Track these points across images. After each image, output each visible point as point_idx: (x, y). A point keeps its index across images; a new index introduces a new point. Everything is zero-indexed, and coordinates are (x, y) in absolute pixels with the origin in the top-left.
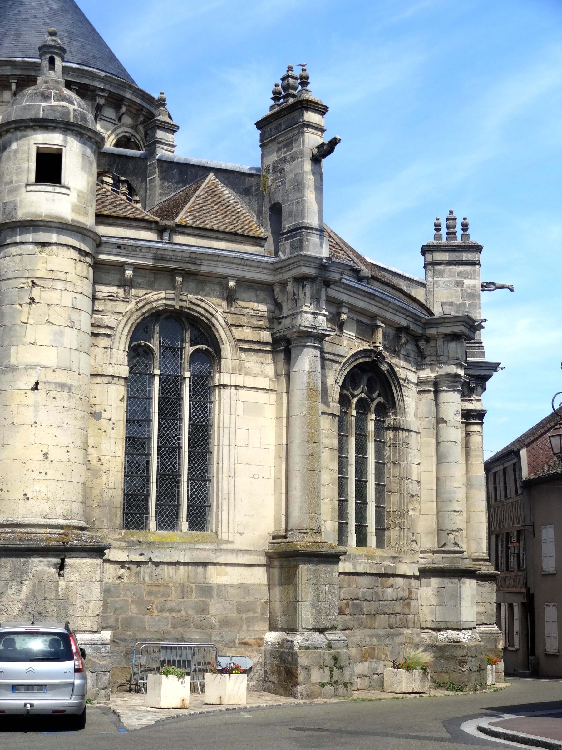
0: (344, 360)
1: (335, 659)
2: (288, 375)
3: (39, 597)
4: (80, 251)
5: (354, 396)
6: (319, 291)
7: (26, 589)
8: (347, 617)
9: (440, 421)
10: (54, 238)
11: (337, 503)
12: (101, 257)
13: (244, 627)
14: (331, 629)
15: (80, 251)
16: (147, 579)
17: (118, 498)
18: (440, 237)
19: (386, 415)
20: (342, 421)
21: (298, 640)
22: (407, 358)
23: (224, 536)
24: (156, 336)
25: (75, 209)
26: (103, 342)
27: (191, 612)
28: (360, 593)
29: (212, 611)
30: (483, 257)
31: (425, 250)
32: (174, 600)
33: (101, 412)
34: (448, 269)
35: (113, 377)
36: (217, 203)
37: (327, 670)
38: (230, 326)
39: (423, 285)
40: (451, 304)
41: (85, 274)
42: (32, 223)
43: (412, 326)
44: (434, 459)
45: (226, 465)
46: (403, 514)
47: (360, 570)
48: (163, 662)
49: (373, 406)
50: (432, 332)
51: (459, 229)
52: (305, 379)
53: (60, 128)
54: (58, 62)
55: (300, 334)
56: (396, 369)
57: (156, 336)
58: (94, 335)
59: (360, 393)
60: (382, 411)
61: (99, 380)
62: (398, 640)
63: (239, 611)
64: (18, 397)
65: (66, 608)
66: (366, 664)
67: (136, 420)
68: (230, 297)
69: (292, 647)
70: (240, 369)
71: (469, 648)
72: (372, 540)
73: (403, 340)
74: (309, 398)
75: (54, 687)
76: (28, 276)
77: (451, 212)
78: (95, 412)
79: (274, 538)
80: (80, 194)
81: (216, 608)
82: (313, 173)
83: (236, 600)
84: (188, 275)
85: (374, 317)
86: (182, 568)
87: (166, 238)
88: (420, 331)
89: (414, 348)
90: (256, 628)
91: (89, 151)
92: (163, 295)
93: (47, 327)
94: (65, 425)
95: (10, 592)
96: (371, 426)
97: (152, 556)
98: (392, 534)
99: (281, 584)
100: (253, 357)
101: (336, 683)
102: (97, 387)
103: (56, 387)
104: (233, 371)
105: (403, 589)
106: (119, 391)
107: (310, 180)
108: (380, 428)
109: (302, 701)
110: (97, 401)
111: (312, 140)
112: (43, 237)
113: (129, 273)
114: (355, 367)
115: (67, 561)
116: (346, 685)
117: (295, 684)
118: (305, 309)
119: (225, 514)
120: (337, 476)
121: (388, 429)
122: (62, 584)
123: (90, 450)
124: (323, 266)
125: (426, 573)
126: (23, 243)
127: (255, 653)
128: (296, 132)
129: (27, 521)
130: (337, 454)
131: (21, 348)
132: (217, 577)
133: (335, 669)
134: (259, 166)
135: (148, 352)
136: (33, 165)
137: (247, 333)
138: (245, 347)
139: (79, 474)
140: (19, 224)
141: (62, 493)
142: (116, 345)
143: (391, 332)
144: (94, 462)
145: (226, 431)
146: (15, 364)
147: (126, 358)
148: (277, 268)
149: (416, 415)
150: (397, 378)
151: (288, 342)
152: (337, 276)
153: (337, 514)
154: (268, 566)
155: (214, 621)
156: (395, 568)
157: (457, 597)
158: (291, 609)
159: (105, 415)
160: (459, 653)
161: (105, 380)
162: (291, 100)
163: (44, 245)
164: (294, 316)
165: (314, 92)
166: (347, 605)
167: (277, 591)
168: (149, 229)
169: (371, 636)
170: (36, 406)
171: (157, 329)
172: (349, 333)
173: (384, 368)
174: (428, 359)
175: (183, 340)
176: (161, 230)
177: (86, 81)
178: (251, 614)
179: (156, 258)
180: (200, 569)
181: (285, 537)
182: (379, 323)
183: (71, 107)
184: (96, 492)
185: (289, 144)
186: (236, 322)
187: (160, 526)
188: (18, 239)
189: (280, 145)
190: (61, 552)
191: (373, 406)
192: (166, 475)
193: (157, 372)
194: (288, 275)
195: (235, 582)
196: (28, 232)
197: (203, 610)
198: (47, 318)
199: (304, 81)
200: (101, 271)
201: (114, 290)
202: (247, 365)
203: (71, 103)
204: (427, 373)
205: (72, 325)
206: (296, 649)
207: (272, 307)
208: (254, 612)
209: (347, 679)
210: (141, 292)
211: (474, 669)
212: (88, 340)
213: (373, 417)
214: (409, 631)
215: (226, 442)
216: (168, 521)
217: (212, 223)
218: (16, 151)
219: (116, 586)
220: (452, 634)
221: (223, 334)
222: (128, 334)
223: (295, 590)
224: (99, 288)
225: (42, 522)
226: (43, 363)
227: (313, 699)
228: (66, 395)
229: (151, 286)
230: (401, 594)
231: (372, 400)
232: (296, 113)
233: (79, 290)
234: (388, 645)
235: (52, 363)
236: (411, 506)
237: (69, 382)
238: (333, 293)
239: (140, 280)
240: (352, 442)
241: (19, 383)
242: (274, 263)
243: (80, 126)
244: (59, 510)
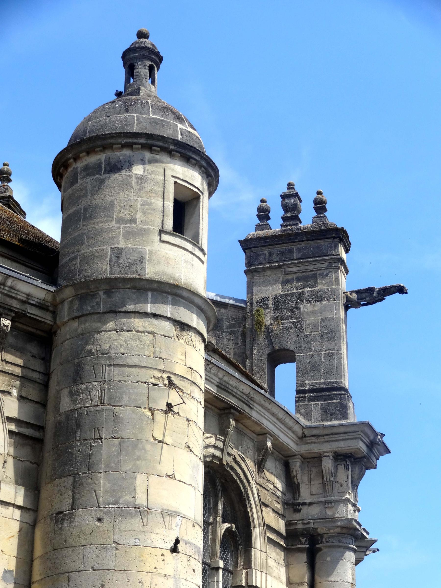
42: (175, 291)
55: (344, 531)
76: (162, 368)
126: (155, 316)
128: (323, 266)
131: (153, 479)
140: (155, 286)
146: (145, 503)
185: (309, 279)
188: (150, 308)
189: (290, 277)
194: (328, 448)
196: (164, 302)
198: (186, 440)
218: (141, 179)
241: (153, 536)
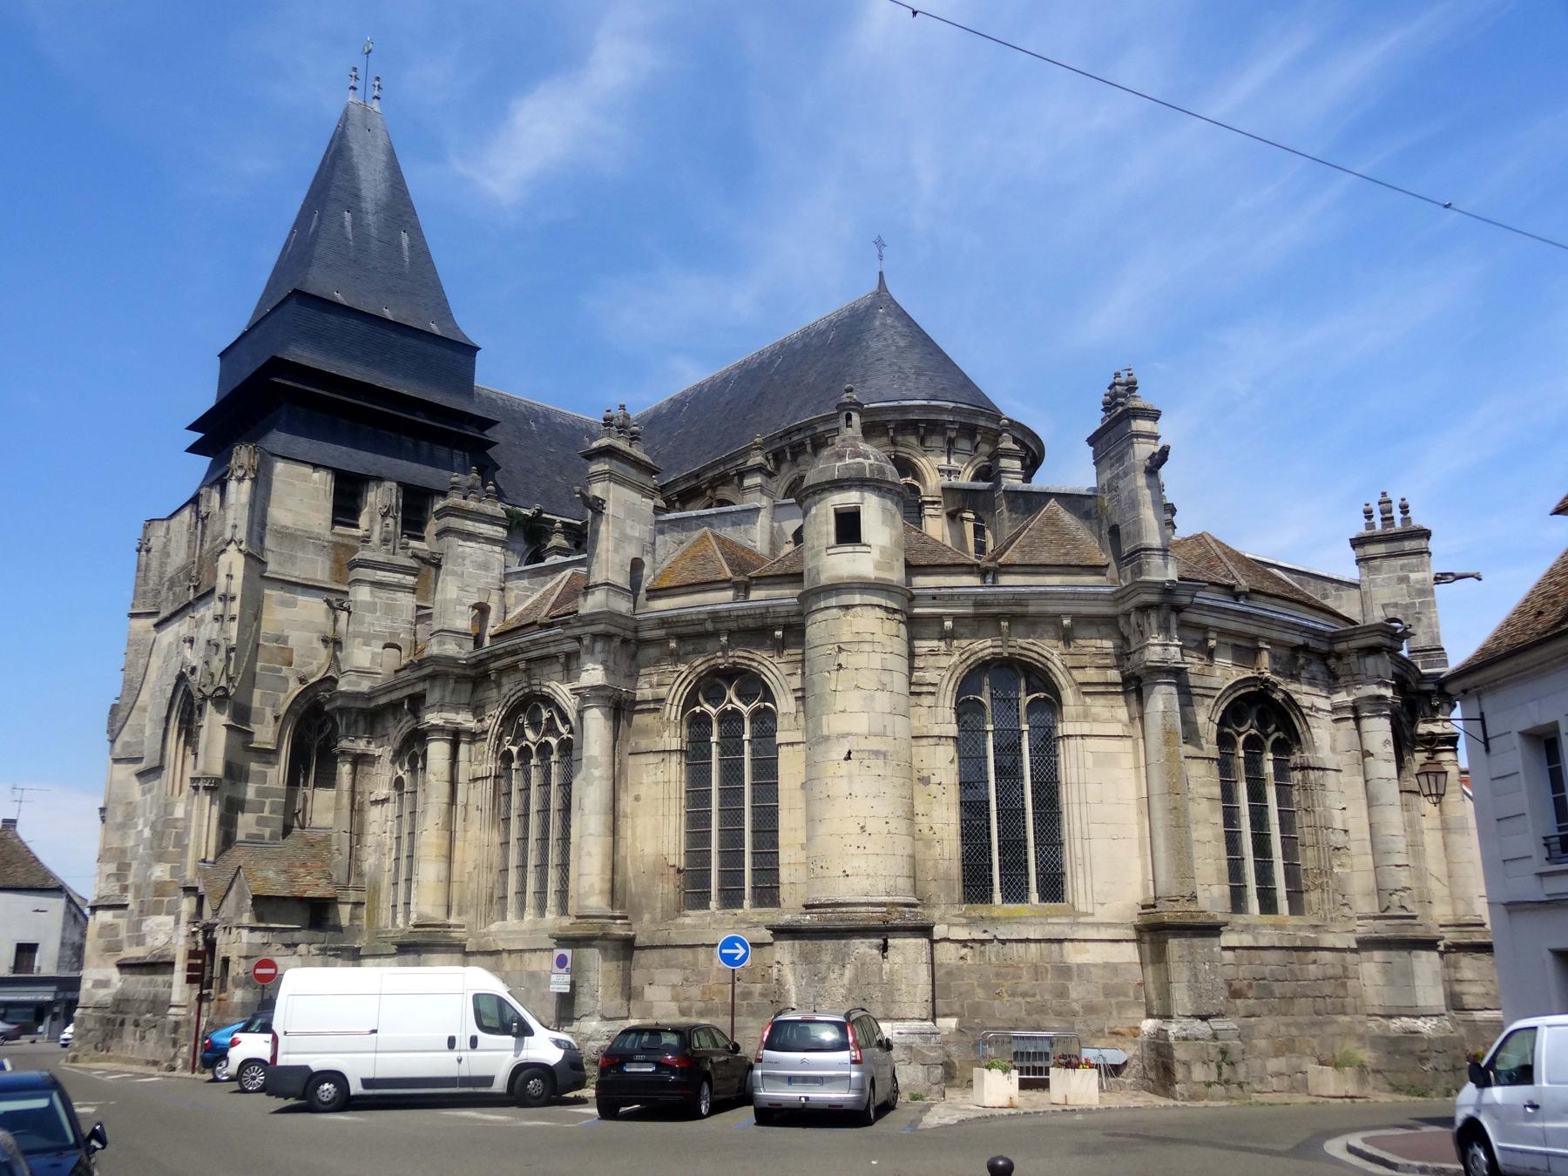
0: (1218, 694)
1: (1224, 1052)
2: (1142, 718)
3: (863, 981)
4: (886, 609)
5: (1240, 734)
6: (1167, 620)
7: (849, 972)
8: (1252, 1001)
9: (1366, 754)
10: (857, 599)
11: (1225, 863)
12: (917, 610)
13: (1115, 1013)
14: (1217, 1016)
15: (886, 609)
17: (955, 869)
18: (1371, 526)
19: (1290, 752)
20: (1225, 766)
21: (1173, 1029)
22: (1312, 681)
23: (1081, 906)
24: (987, 688)
25: (878, 566)
26: (927, 701)
27: (1047, 997)
28: (1267, 971)
29: (1073, 995)
30: (1432, 545)
31: (1357, 543)
32: (1026, 982)
34: (1386, 563)
35: (940, 737)
36: (1054, 533)
37: (1213, 1066)
38: (1070, 669)
39: (1356, 586)
40: (1396, 605)
41: (894, 632)
43: (1312, 643)
44: (1364, 802)
45: (1077, 826)
46: (1325, 872)
47: (1263, 942)
48: (1016, 1054)
49: (1269, 744)
50: (1341, 647)
51: (1397, 514)
52: (1160, 721)
54: (856, 418)
56: (1295, 696)
57: (987, 688)
58: (912, 693)
59: (1249, 729)
60: (1282, 748)
61: (924, 742)
62: (1329, 1030)
63: (1106, 995)
64: (831, 769)
65: (891, 994)
66: (1282, 1060)
67: (970, 783)
68: (1067, 637)
69: (1167, 1039)
70: (1085, 716)
71: (1430, 1040)
72: (1283, 905)
73: (1301, 661)
74: (1167, 743)
75: (831, 1079)
77: (1384, 494)
79: (1144, 907)
80: (883, 550)
81: (1077, 992)
82: (1149, 487)
83: (1101, 981)
84: (1013, 618)
85: (1255, 638)
86: (1033, 945)
87: (989, 580)
88: (1325, 648)
89: (1323, 668)
90: (1130, 1014)
91: (889, 504)
92: (989, 643)
93: (857, 693)
95: (832, 976)
96: (1269, 768)
98: (1312, 897)
99: (1153, 963)
100: (1101, 701)
101: (1227, 1082)
102: (924, 750)
104: (1077, 719)
105: (1333, 966)
106: (948, 751)
107: (1146, 495)
108: (1281, 770)
109: (1180, 1103)
110: (924, 765)
111: (1143, 451)
112: (846, 599)
113: (948, 624)
114: (1236, 699)
115: (890, 941)
116: (1240, 1085)
117: (1173, 1082)
118: (1151, 641)
119: (1081, 881)
120: (1222, 830)
121: (1294, 769)
122: (886, 966)
123: (919, 819)
124: (1167, 590)
125: (1366, 944)
127: (1129, 1045)
129: (848, 899)
130: (1220, 805)
131: (832, 716)
132: (1075, 955)
133: (1224, 1065)
134: (1094, 485)
136: (831, 527)
137: (1091, 675)
138: (1087, 690)
139: (902, 846)
142: (941, 703)
143: (1285, 653)
144: (926, 831)
145: (1075, 787)
148: (1118, 598)
149: (1333, 749)
150: (1298, 708)
151: (1139, 679)
152: (1186, 600)
153: (1226, 877)
154: (1139, 941)
155: (1076, 1007)
156: (1316, 939)
157: (1409, 974)
158: (1165, 991)
159: (934, 779)
160: (1418, 1047)
161: (932, 741)
162: (1120, 409)
163: (848, 607)
164: (1142, 649)
165: (1143, 399)
166: (1250, 986)
167: (1150, 970)
168: (971, 573)
169: (1288, 1025)
170: (850, 777)
171: (987, 680)
172: (1223, 661)
173: (1278, 696)
174: (1342, 680)
175: (1018, 690)
176: (983, 573)
177: (933, 417)
178: (1122, 999)
179: (976, 604)
180: (1055, 947)
181: (1154, 906)
182: (1262, 645)
183: (866, 462)
184: (930, 864)
185: (1120, 459)
186: (1074, 664)
187: (1006, 898)
188: (822, 604)
190: (883, 932)
191: (1269, 744)
192: (1010, 842)
193: (990, 727)
195: (1100, 961)
197: (1062, 993)
199: (1131, 387)
200: (915, 626)
201: (935, 643)
202: (1094, 710)
203: (868, 458)
204: (1342, 698)
205: (883, 687)
206: (1172, 1040)
207: (1119, 642)
208: (1126, 995)
209: (1241, 1077)
210: (964, 643)
211: (1442, 1067)
212: (903, 701)
213: (1270, 756)
214: (1347, 1019)
215: (1076, 800)
216: (1016, 892)
217: (1044, 558)
219: (959, 968)
220: (1406, 1022)
221: (1062, 679)
223: (1167, 970)
224: (917, 643)
225: (863, 899)
226: (854, 731)
227: (1197, 1099)
228: (880, 762)
229: (975, 635)
230: (1330, 972)
231: (1267, 736)
232: (1123, 425)
234: (1314, 1036)
235: (864, 729)
236: (1335, 862)
237: (884, 748)
238: (1193, 617)
239: (962, 630)
240: (1242, 790)
242: (1112, 594)
243: (877, 480)
244: (881, 887)
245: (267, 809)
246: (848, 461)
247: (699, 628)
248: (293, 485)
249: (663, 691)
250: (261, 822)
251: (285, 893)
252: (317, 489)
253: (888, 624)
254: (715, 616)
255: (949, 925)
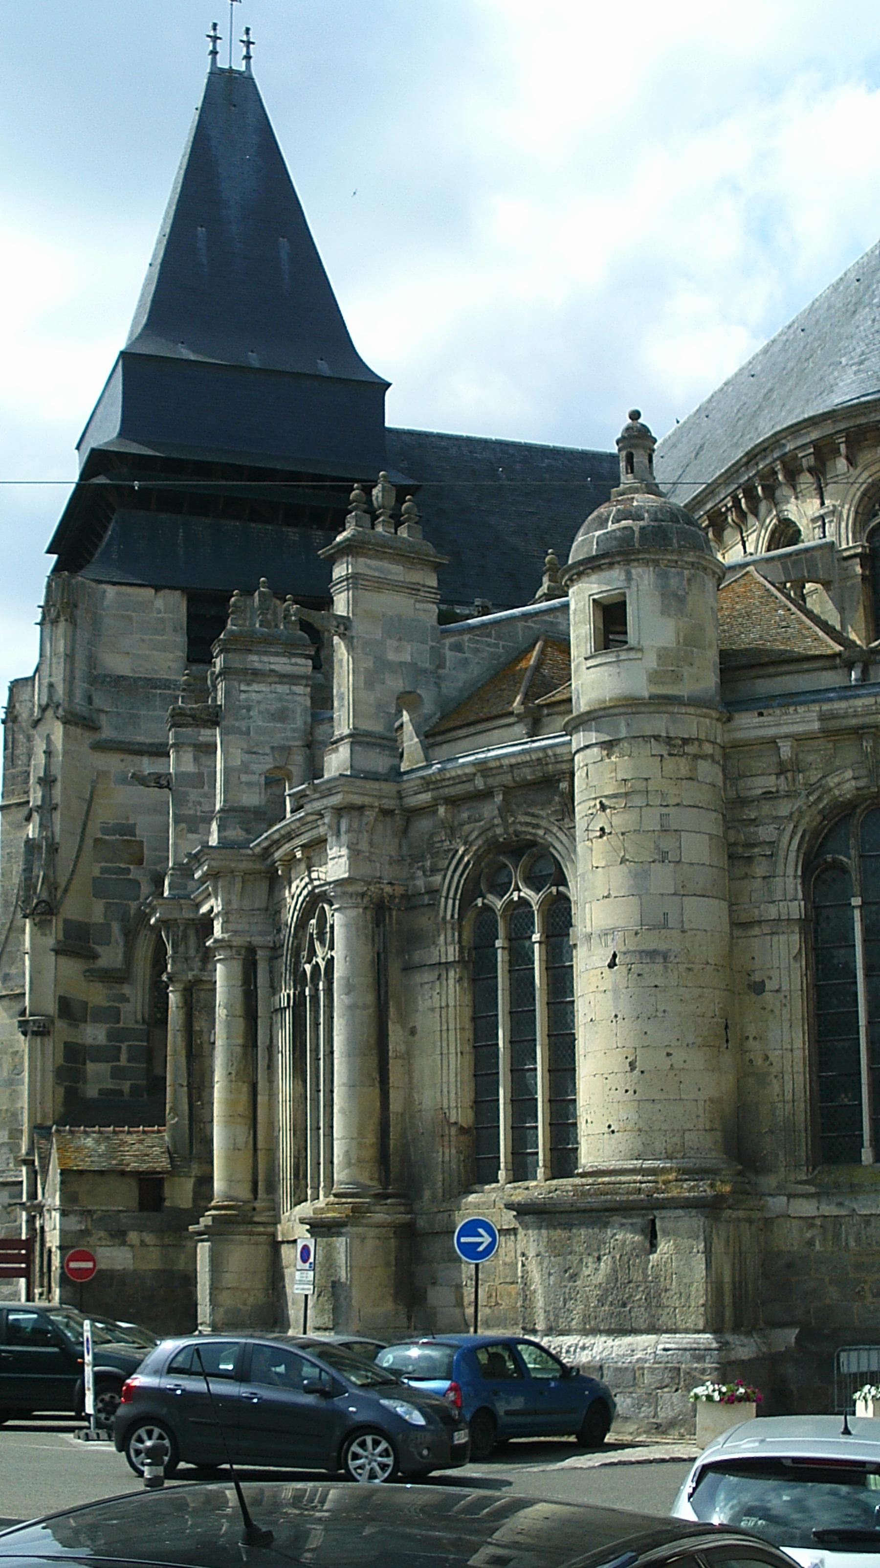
7: (605, 1266)
16: (852, 1244)
25: (654, 678)
33: (763, 981)
41: (684, 771)
42: (592, 716)
53: (618, 563)
61: (756, 931)
78: (755, 983)
80: (663, 655)
94: (660, 1014)
97: (856, 1207)
102: (756, 943)
103: (641, 958)
135: (843, 869)
141: (663, 1118)
142: (780, 870)
144: (759, 1062)
147: (799, 888)
159: (769, 986)
222: (799, 848)
228: (659, 968)
233: (673, 801)
237: (663, 947)
245: (124, 1057)
246: (611, 527)
247: (468, 787)
248: (130, 618)
249: (438, 878)
250: (118, 1074)
251: (104, 1165)
252: (162, 621)
253: (670, 764)
254: (483, 768)
255: (790, 1196)
